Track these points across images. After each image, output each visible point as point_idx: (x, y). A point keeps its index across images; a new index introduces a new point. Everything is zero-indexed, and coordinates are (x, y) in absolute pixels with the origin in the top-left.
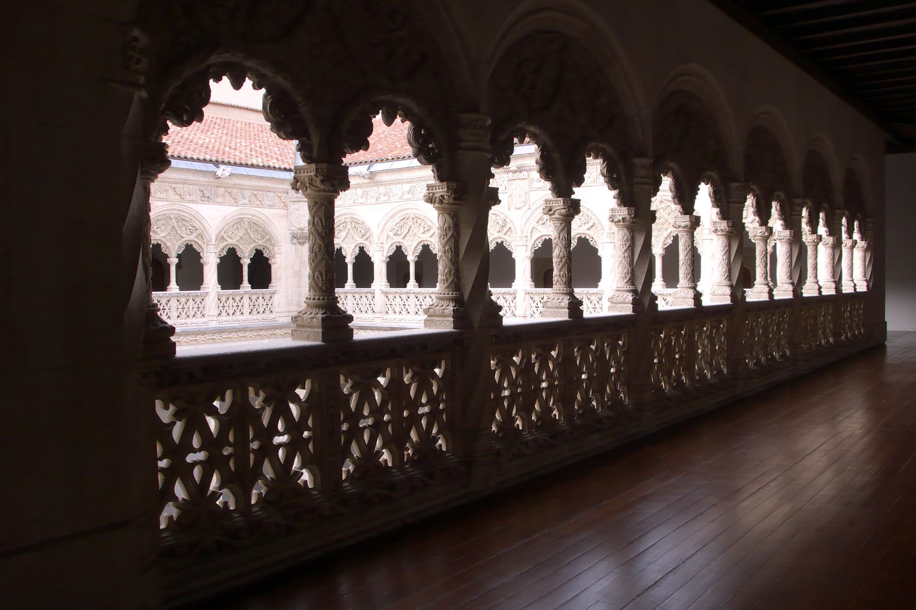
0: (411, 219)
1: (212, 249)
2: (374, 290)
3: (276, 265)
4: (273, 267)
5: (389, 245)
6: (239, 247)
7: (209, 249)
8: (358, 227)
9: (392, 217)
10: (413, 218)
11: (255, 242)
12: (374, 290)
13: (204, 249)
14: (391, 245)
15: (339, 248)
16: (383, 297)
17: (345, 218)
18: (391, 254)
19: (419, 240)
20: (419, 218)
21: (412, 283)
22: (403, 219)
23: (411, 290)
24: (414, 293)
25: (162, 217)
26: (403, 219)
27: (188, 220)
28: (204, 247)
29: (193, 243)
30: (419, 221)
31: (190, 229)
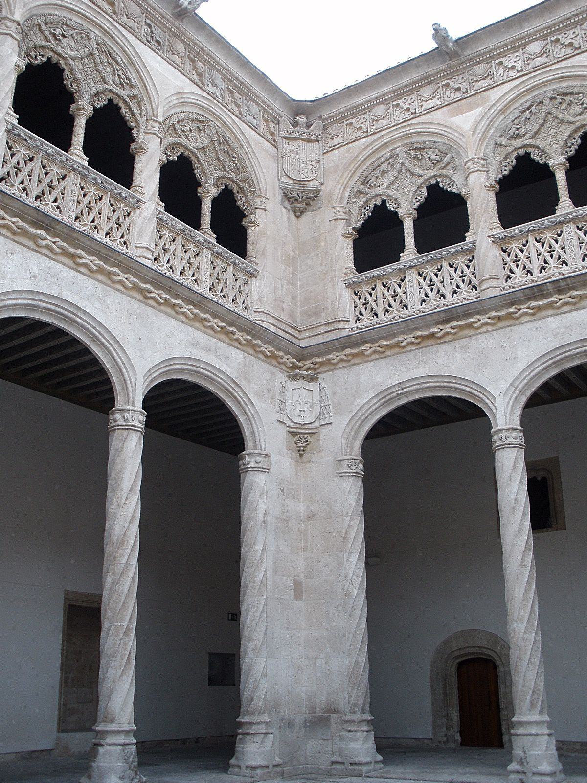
0: (546, 101)
1: (157, 129)
2: (475, 241)
3: (257, 228)
4: (250, 231)
5: (499, 158)
6: (199, 161)
7: (149, 127)
8: (423, 153)
9: (503, 111)
10: (552, 99)
11: (225, 170)
12: (475, 241)
13: (141, 126)
14: (505, 158)
15: (379, 203)
16: (496, 251)
17: (392, 150)
18: (506, 173)
19: (574, 127)
20: (566, 94)
21: (565, 206)
22: (528, 109)
23: (567, 214)
24: (574, 220)
25: (76, 26)
26: (528, 109)
29: (121, 104)
30: (569, 98)
31: (118, 75)
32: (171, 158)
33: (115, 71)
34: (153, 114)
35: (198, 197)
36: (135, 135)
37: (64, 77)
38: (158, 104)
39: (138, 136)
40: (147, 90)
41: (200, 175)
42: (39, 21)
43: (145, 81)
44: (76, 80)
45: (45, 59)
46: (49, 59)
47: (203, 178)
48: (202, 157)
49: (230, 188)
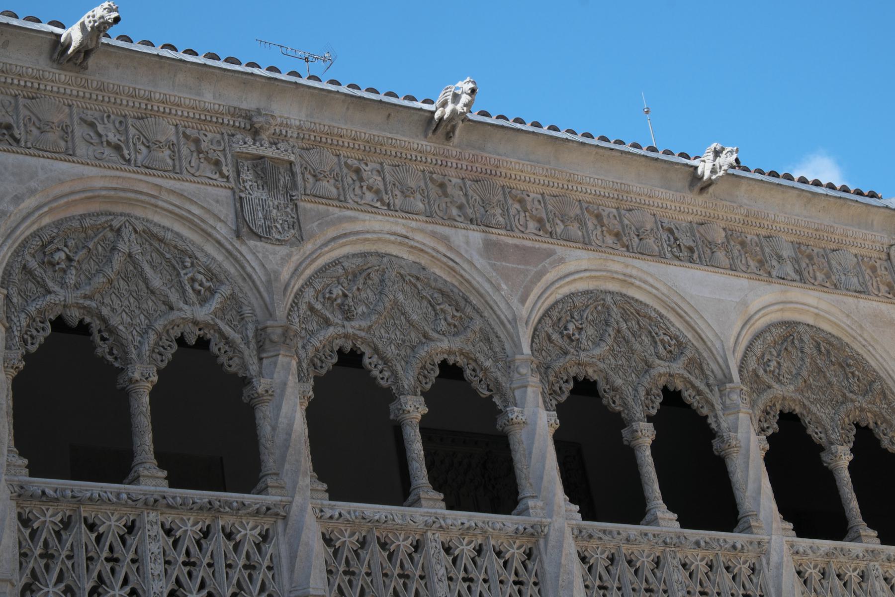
13: (716, 406)
27: (653, 314)
28: (715, 399)
32: (770, 432)
33: (653, 337)
34: (724, 375)
35: (826, 468)
36: (714, 426)
37: (601, 394)
38: (725, 355)
39: (719, 426)
40: (702, 339)
41: (816, 433)
42: (546, 329)
43: (696, 327)
44: (615, 389)
45: (571, 385)
46: (575, 379)
47: (822, 435)
48: (808, 398)
49: (863, 424)
